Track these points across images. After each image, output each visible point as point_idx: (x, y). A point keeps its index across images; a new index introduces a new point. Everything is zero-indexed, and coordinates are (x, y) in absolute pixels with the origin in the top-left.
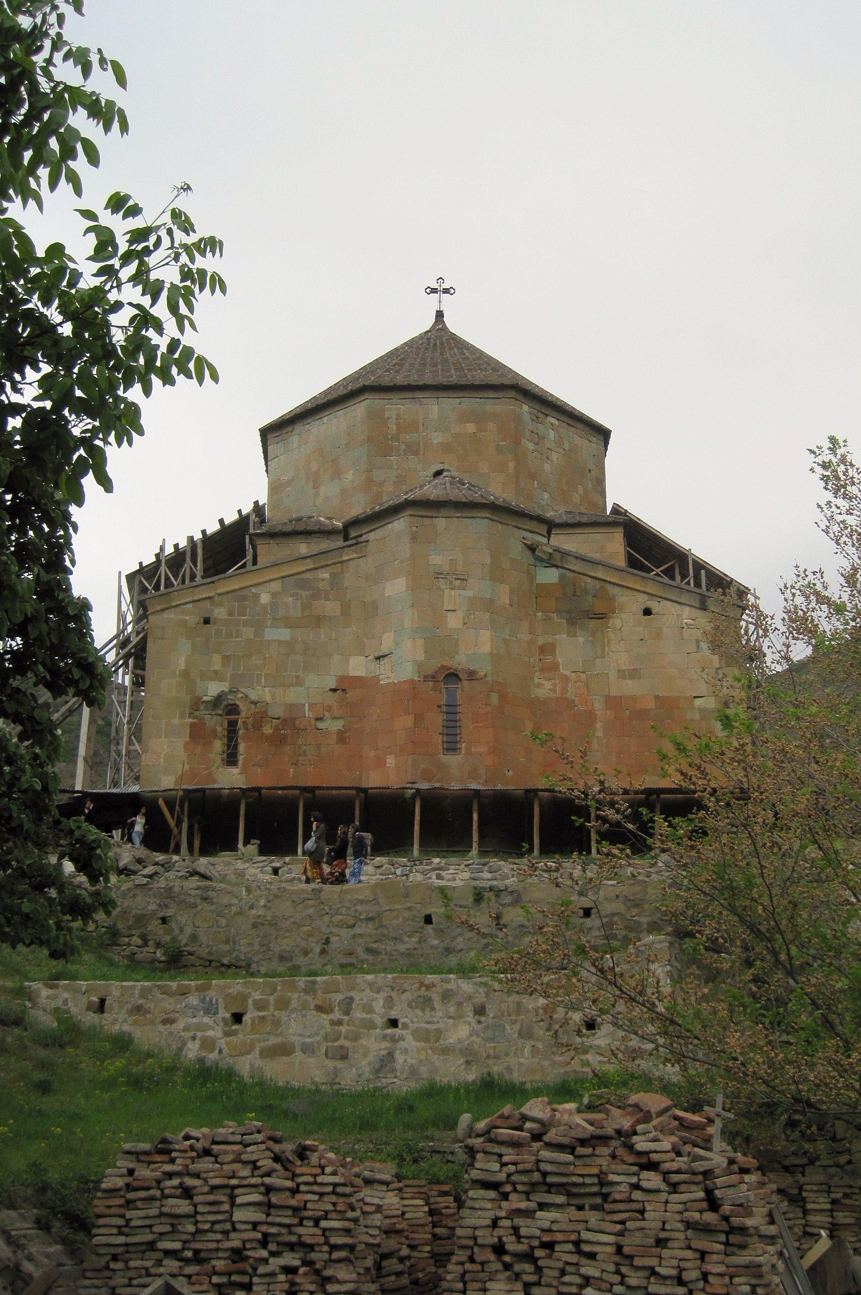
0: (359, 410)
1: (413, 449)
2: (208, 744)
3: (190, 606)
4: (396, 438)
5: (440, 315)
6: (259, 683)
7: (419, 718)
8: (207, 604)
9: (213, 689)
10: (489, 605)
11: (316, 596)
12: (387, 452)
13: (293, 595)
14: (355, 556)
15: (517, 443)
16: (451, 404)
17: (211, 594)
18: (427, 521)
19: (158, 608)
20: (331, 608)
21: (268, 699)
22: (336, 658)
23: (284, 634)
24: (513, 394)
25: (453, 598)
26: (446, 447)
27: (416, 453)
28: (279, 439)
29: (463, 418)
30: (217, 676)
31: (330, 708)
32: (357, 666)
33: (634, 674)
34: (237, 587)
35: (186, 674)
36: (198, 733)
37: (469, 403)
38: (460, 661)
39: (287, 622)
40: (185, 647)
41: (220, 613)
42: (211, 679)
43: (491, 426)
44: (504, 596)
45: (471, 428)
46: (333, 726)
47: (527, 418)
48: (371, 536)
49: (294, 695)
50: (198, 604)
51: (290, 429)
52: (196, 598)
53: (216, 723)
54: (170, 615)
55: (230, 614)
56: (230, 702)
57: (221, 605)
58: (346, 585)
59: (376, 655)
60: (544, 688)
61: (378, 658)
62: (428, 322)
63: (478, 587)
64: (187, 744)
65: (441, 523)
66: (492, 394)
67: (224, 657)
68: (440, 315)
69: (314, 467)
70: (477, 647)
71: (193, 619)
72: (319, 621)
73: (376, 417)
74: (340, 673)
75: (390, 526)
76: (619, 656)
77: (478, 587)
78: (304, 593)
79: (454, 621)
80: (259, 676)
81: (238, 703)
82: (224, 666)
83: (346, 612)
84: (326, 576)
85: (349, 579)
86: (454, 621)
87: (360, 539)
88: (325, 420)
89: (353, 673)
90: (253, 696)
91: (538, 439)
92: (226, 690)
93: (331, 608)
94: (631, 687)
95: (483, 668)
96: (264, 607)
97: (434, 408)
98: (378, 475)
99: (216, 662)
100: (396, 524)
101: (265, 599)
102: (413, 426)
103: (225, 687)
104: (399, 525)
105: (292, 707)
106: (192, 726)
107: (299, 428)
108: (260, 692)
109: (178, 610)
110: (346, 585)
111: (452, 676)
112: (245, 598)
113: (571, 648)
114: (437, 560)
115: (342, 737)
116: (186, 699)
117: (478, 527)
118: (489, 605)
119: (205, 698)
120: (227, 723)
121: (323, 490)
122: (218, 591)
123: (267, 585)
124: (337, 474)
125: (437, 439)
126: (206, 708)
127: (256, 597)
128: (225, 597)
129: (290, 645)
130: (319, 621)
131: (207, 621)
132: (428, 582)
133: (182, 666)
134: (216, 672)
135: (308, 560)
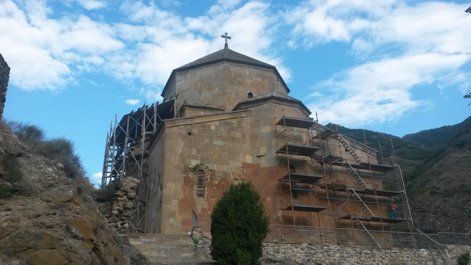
0: (220, 67)
1: (241, 84)
2: (192, 186)
3: (183, 126)
4: (235, 78)
5: (226, 45)
6: (212, 162)
8: (190, 127)
9: (194, 163)
11: (232, 129)
13: (224, 128)
14: (245, 115)
17: (192, 123)
18: (278, 105)
19: (170, 126)
20: (238, 135)
21: (216, 169)
22: (241, 155)
23: (221, 143)
24: (273, 70)
26: (252, 85)
27: (242, 85)
28: (181, 74)
29: (257, 76)
30: (195, 157)
31: (240, 175)
32: (249, 159)
34: (202, 121)
35: (182, 155)
37: (258, 71)
39: (222, 138)
40: (181, 143)
41: (195, 131)
42: (193, 159)
45: (260, 80)
47: (276, 80)
48: (252, 109)
49: (225, 168)
50: (187, 126)
51: (187, 71)
52: (185, 124)
54: (174, 129)
55: (199, 132)
56: (201, 169)
57: (196, 128)
58: (243, 126)
59: (258, 155)
61: (259, 157)
62: (223, 47)
64: (183, 186)
66: (266, 69)
67: (197, 150)
68: (226, 45)
69: (199, 85)
71: (184, 133)
74: (243, 161)
75: (262, 106)
78: (227, 127)
80: (212, 159)
81: (204, 170)
82: (197, 153)
83: (243, 137)
84: (236, 122)
87: (248, 109)
88: (204, 69)
89: (248, 162)
90: (210, 168)
92: (199, 163)
96: (213, 131)
99: (194, 152)
100: (265, 105)
101: (213, 128)
103: (198, 162)
105: (225, 173)
106: (185, 178)
107: (191, 71)
109: (178, 127)
110: (243, 126)
112: (204, 127)
116: (182, 166)
119: (190, 166)
121: (203, 94)
122: (195, 122)
123: (213, 122)
124: (211, 89)
125: (249, 81)
126: (191, 171)
127: (209, 127)
128: (197, 125)
130: (234, 139)
131: (190, 134)
133: (180, 151)
134: (194, 156)
135: (229, 115)
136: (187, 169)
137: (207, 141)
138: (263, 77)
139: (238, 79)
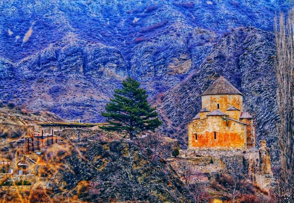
12: (212, 102)
23: (201, 127)
25: (215, 124)
26: (219, 101)
29: (220, 98)
32: (207, 130)
33: (233, 131)
38: (215, 131)
40: (192, 129)
41: (195, 125)
43: (224, 98)
44: (220, 124)
45: (221, 99)
70: (217, 129)
71: (192, 126)
73: (211, 97)
76: (231, 129)
85: (206, 121)
93: (204, 124)
94: (232, 132)
97: (217, 96)
102: (215, 99)
104: (210, 117)
105: (202, 135)
125: (218, 100)
129: (201, 128)
137: (197, 127)
138: (222, 97)
139: (215, 100)
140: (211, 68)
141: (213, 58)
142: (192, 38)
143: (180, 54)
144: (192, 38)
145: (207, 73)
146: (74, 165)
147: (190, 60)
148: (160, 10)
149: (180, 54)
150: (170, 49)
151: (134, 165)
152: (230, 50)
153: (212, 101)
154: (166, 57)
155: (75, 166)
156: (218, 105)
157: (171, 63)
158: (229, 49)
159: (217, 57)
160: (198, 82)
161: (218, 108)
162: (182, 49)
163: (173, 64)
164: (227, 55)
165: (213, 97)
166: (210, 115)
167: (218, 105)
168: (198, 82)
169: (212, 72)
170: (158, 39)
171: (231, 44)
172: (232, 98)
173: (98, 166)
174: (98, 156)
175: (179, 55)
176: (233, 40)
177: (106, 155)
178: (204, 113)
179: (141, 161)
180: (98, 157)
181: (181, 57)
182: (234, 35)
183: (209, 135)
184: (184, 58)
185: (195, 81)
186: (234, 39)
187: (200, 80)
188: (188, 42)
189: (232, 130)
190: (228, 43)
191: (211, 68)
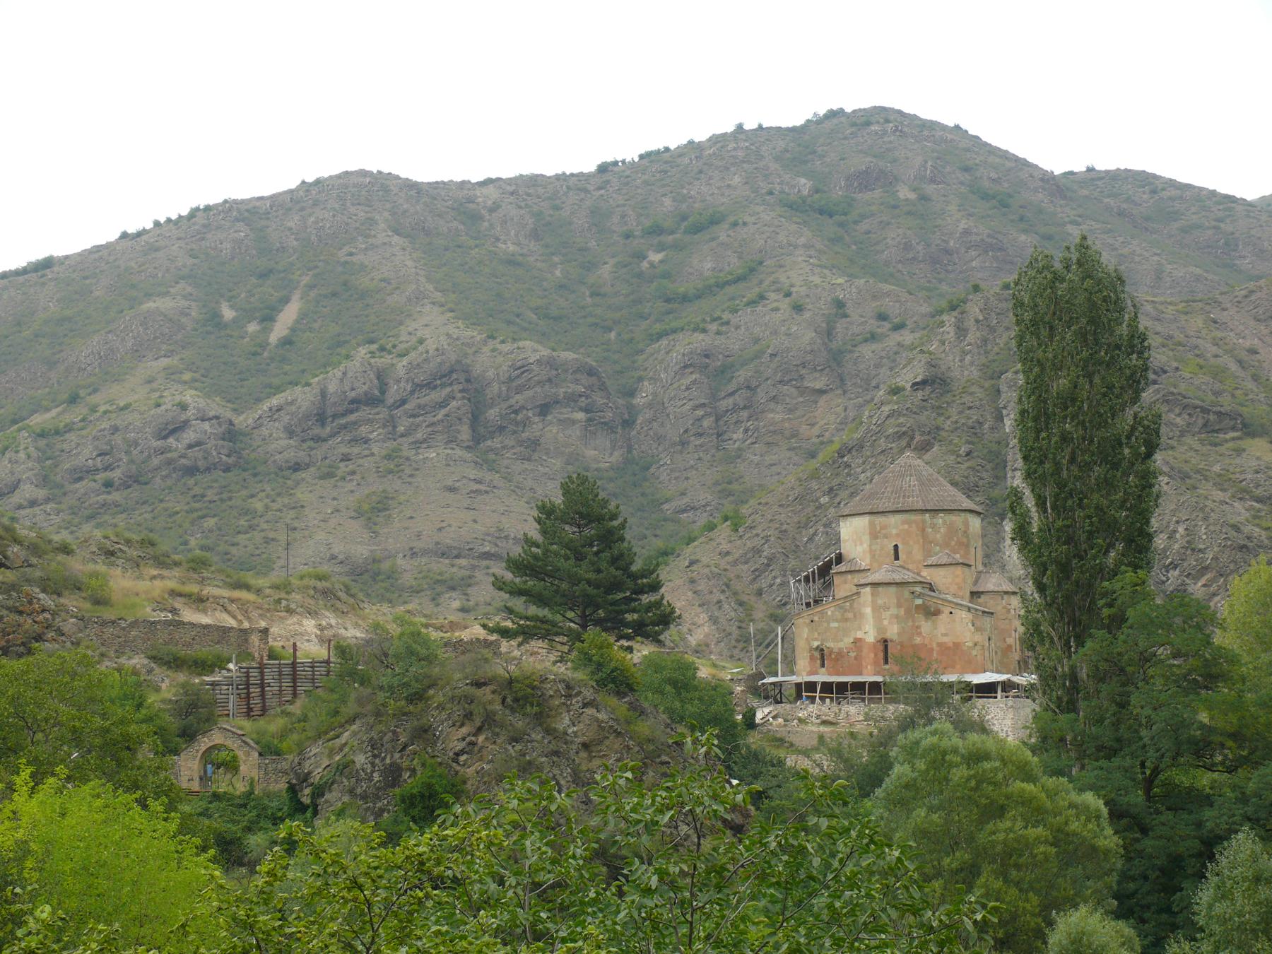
7: (876, 655)
9: (816, 644)
10: (897, 617)
15: (923, 530)
16: (899, 517)
20: (850, 615)
23: (836, 625)
26: (898, 535)
29: (904, 523)
30: (816, 639)
32: (860, 635)
33: (946, 635)
36: (812, 658)
38: (888, 635)
39: (837, 621)
40: (806, 630)
41: (816, 618)
44: (902, 612)
45: (906, 527)
46: (852, 654)
49: (841, 645)
53: (817, 655)
60: (918, 640)
63: (894, 611)
65: (880, 589)
70: (893, 632)
71: (808, 621)
72: (847, 620)
73: (872, 524)
77: (894, 611)
79: (886, 622)
85: (855, 605)
86: (886, 622)
91: (933, 526)
93: (850, 615)
94: (945, 639)
95: (895, 637)
97: (894, 520)
98: (874, 547)
99: (816, 635)
104: (868, 589)
105: (840, 649)
108: (830, 644)
111: (886, 641)
113: (925, 626)
114: (880, 602)
115: (856, 658)
117: (893, 590)
118: (897, 617)
120: (821, 656)
125: (894, 531)
130: (847, 620)
132: (877, 609)
136: (811, 649)
140: (901, 420)
141: (908, 386)
142: (846, 316)
143: (803, 372)
144: (846, 316)
145: (887, 437)
146: (384, 759)
147: (839, 391)
148: (735, 224)
149: (803, 372)
150: (771, 355)
151: (583, 754)
152: (968, 358)
153: (874, 535)
154: (754, 384)
155: (388, 761)
156: (896, 546)
157: (772, 405)
158: (964, 353)
159: (924, 382)
160: (859, 470)
161: (897, 558)
162: (809, 357)
163: (780, 408)
164: (956, 373)
165: (880, 520)
166: (867, 585)
167: (896, 546)
168: (859, 470)
169: (904, 433)
170: (728, 323)
171: (970, 338)
172: (944, 522)
173: (463, 758)
174: (462, 725)
175: (802, 378)
176: (977, 321)
177: (489, 722)
178: (849, 576)
179: (607, 742)
180: (464, 730)
181: (806, 384)
182: (981, 303)
183: (865, 651)
184: (818, 385)
185: (848, 466)
186: (981, 318)
187: (864, 463)
188: (829, 333)
189: (943, 631)
190: (961, 331)
191: (901, 420)
